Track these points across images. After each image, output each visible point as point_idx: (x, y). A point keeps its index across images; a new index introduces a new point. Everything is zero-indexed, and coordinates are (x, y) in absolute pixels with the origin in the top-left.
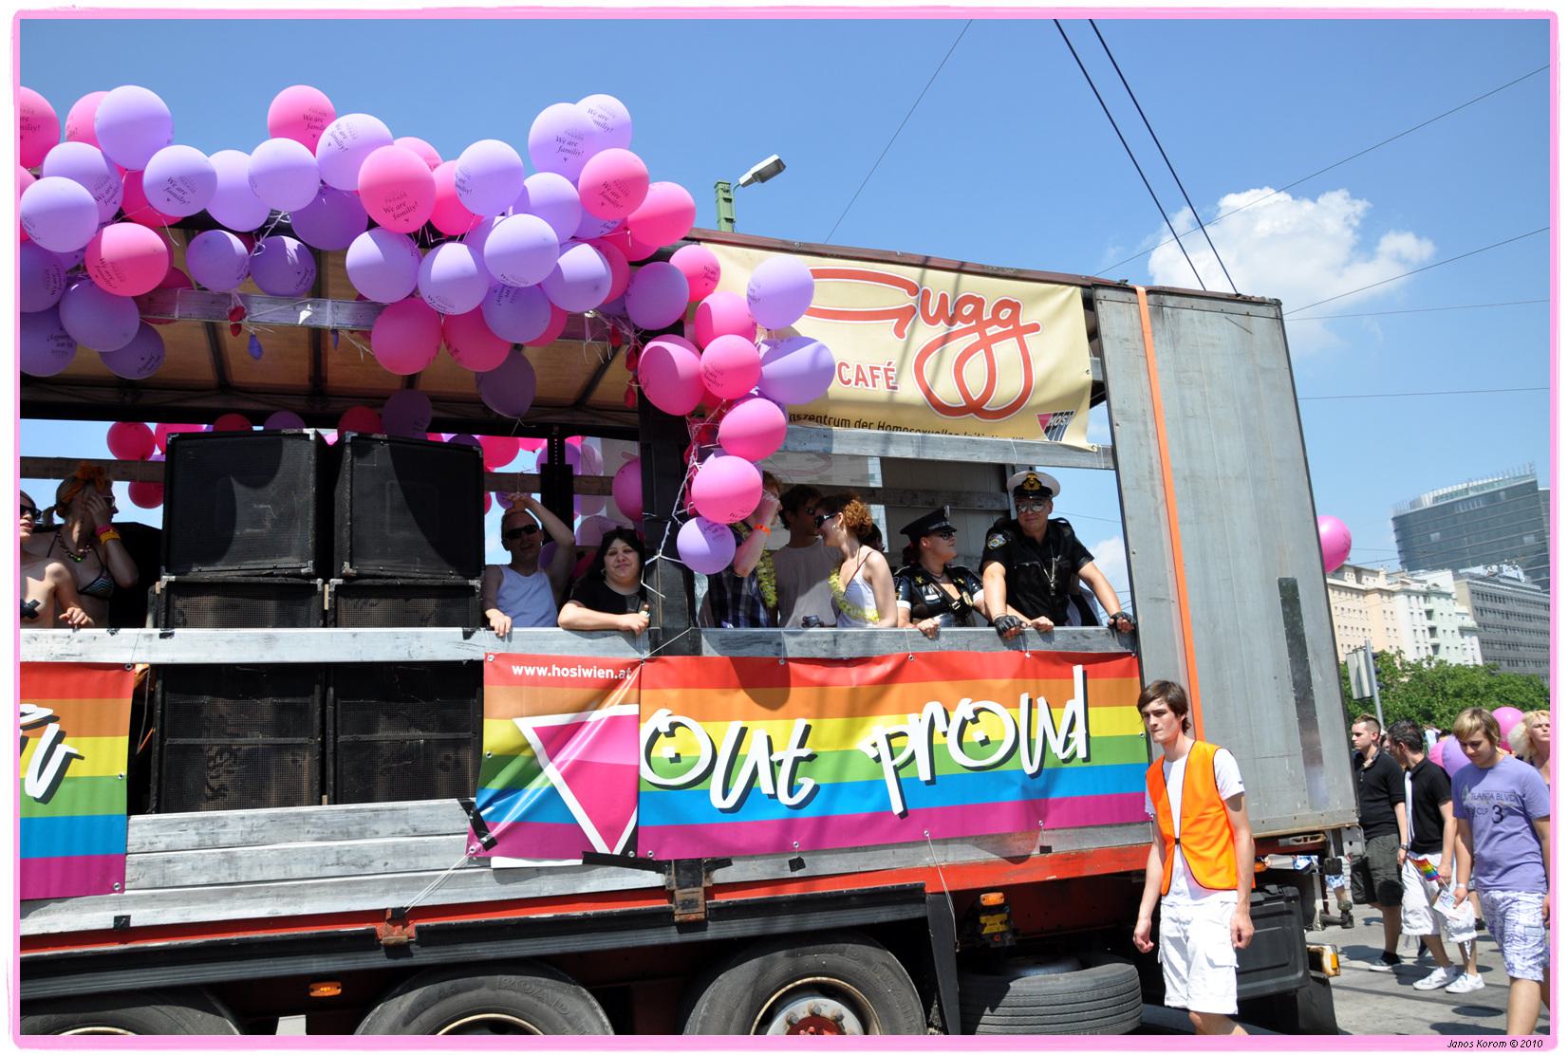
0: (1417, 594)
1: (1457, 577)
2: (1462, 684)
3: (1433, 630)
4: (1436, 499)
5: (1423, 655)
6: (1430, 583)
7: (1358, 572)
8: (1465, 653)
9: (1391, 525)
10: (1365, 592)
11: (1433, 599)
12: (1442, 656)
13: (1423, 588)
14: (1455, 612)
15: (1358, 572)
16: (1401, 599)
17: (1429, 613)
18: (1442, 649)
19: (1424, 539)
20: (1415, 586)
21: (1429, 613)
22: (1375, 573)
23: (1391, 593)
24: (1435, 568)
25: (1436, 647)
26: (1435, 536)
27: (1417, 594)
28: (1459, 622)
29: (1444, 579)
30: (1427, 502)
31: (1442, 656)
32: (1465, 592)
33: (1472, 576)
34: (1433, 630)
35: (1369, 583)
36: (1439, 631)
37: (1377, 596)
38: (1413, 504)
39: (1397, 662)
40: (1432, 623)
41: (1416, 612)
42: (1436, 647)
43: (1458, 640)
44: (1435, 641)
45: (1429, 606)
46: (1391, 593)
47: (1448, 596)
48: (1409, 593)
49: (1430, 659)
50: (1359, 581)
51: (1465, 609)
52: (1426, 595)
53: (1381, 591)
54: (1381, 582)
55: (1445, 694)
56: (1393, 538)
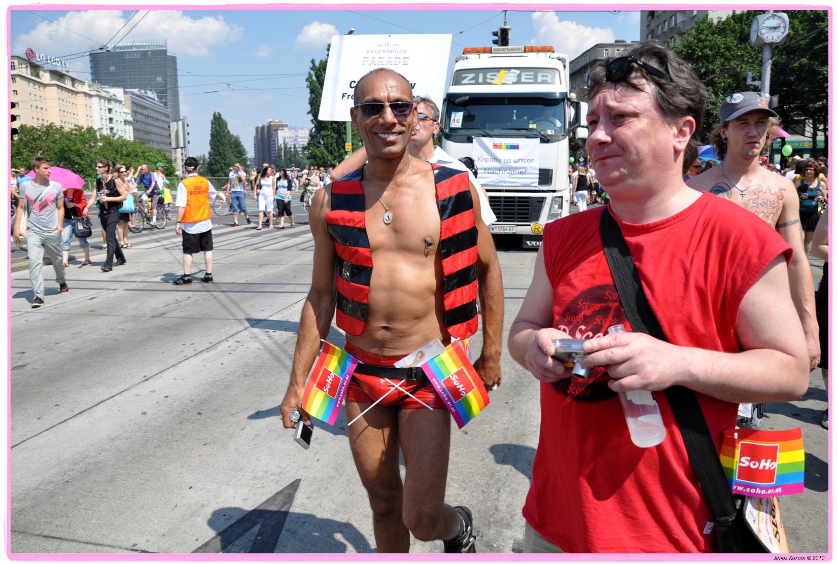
0: (105, 98)
1: (125, 93)
2: (130, 149)
3: (111, 119)
7: (73, 80)
8: (128, 134)
10: (76, 93)
11: (113, 103)
13: (108, 96)
14: (123, 112)
16: (96, 99)
17: (110, 110)
18: (115, 131)
20: (103, 94)
21: (110, 110)
22: (82, 83)
23: (91, 96)
24: (115, 85)
25: (111, 129)
27: (105, 98)
28: (122, 118)
29: (118, 92)
32: (129, 103)
33: (133, 94)
34: (111, 119)
35: (78, 88)
36: (114, 121)
40: (111, 116)
41: (103, 108)
42: (111, 129)
44: (111, 125)
45: (110, 106)
46: (91, 96)
47: (120, 102)
48: (100, 97)
50: (73, 86)
51: (128, 111)
52: (109, 100)
53: (86, 94)
54: (86, 89)
55: (122, 154)
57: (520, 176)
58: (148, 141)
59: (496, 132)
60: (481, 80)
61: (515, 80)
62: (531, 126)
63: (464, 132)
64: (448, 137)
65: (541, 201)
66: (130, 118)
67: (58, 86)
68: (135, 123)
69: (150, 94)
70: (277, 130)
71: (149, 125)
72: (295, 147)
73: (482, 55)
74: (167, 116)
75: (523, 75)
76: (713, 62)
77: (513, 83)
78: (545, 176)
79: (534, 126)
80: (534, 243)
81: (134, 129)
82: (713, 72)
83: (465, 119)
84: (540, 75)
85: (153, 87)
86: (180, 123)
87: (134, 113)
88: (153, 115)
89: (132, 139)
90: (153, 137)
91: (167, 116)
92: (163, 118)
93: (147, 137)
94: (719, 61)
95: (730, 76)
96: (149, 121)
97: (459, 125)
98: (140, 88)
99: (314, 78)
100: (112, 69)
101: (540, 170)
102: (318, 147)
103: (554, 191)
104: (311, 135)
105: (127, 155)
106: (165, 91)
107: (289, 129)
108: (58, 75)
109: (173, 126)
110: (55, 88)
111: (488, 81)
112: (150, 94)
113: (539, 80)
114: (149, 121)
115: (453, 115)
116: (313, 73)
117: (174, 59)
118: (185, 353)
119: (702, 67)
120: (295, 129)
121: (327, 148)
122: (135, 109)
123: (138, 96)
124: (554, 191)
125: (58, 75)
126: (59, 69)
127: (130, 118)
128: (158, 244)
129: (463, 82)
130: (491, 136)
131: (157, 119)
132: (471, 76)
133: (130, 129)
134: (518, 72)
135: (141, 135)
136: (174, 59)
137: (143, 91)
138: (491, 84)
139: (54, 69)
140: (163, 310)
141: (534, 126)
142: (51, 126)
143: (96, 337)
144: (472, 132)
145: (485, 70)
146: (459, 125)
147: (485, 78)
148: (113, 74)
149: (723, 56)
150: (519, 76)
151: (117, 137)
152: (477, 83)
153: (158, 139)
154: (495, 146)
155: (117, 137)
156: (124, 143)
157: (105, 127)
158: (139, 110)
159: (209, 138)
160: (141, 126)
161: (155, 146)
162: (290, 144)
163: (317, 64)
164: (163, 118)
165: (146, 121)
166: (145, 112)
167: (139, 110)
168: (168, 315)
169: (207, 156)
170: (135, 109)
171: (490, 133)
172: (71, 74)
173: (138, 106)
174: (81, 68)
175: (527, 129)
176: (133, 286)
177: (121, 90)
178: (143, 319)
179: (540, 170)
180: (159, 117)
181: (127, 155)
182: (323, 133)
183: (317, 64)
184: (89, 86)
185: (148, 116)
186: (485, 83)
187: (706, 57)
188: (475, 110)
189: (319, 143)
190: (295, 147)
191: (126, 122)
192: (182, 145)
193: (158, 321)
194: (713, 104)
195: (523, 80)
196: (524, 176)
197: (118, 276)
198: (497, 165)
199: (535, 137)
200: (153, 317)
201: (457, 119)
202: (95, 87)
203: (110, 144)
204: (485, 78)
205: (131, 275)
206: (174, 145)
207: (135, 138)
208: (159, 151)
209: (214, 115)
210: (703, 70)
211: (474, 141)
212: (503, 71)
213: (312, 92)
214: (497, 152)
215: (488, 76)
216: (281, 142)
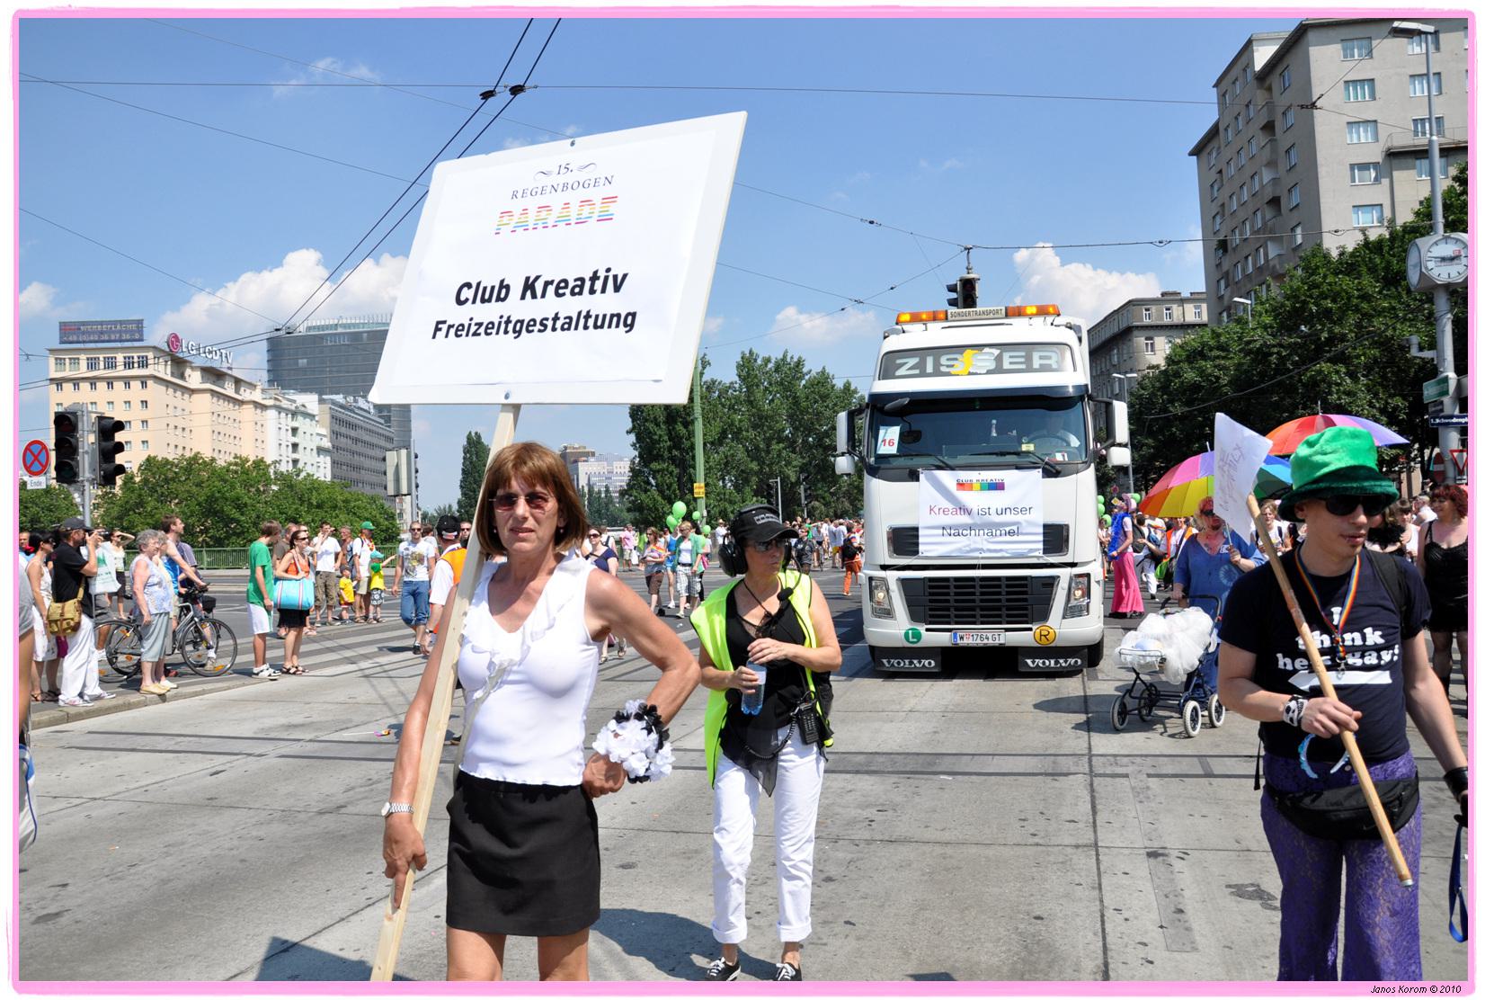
0: (287, 411)
1: (321, 401)
3: (295, 446)
6: (299, 403)
7: (238, 382)
8: (322, 470)
14: (316, 433)
16: (272, 413)
17: (295, 430)
18: (300, 465)
20: (285, 404)
21: (295, 430)
22: (252, 386)
24: (305, 389)
25: (295, 462)
28: (317, 442)
29: (310, 401)
33: (334, 403)
34: (295, 446)
35: (246, 394)
36: (300, 448)
39: (271, 471)
42: (295, 462)
44: (295, 456)
45: (295, 424)
47: (312, 417)
48: (279, 409)
50: (237, 391)
51: (324, 431)
52: (294, 414)
53: (256, 405)
54: (257, 396)
55: (310, 504)
57: (1008, 538)
58: (356, 482)
59: (962, 460)
60: (930, 369)
61: (992, 366)
62: (1024, 448)
63: (902, 462)
64: (874, 472)
65: (1050, 583)
66: (326, 443)
67: (213, 393)
68: (334, 452)
70: (576, 461)
71: (359, 454)
72: (607, 491)
73: (930, 325)
75: (1006, 356)
76: (1340, 322)
77: (989, 372)
78: (1056, 537)
79: (1031, 447)
80: (1039, 662)
81: (333, 462)
82: (1343, 338)
83: (903, 437)
84: (1036, 356)
86: (404, 452)
87: (335, 434)
89: (329, 479)
90: (365, 476)
93: (354, 475)
94: (1352, 319)
95: (1375, 344)
96: (359, 448)
97: (893, 450)
98: (346, 394)
100: (303, 362)
101: (1045, 526)
102: (646, 491)
103: (1073, 565)
104: (632, 470)
105: (319, 506)
107: (598, 460)
109: (391, 457)
110: (208, 396)
111: (943, 369)
113: (1036, 364)
114: (359, 448)
115: (882, 432)
118: (370, 892)
119: (1322, 331)
120: (607, 459)
121: (661, 492)
122: (337, 428)
123: (342, 406)
124: (1073, 565)
126: (216, 365)
127: (326, 443)
128: (353, 667)
129: (898, 373)
130: (952, 468)
131: (372, 445)
132: (913, 361)
133: (326, 461)
134: (996, 352)
135: (344, 471)
137: (351, 399)
138: (948, 374)
139: (208, 364)
140: (341, 799)
141: (1031, 447)
142: (196, 458)
143: (206, 852)
144: (916, 461)
145: (937, 351)
146: (893, 450)
147: (937, 365)
148: (304, 370)
149: (1357, 310)
150: (999, 359)
151: (303, 475)
152: (923, 374)
154: (961, 485)
155: (303, 475)
156: (315, 486)
157: (284, 459)
158: (343, 430)
159: (460, 477)
160: (346, 457)
161: (368, 491)
162: (599, 486)
164: (383, 443)
165: (354, 447)
166: (353, 433)
167: (343, 430)
168: (350, 809)
169: (455, 507)
170: (337, 428)
171: (950, 462)
172: (235, 373)
174: (251, 363)
175: (1018, 454)
176: (295, 748)
177: (315, 397)
178: (302, 816)
179: (1045, 526)
180: (375, 440)
181: (319, 506)
182: (655, 466)
184: (263, 391)
185: (356, 440)
186: (937, 373)
187: (1328, 312)
188: (920, 421)
189: (648, 483)
190: (607, 491)
191: (320, 450)
192: (404, 490)
193: (329, 822)
194: (1348, 394)
195: (1006, 366)
196: (1015, 538)
197: (270, 729)
198: (964, 519)
199: (1033, 466)
200: (320, 813)
201: (889, 439)
202: (272, 393)
203: (291, 487)
204: (937, 365)
205: (295, 726)
206: (391, 491)
207: (334, 476)
208: (373, 499)
209: (469, 437)
210: (1325, 335)
211: (922, 477)
212: (969, 352)
214: (964, 496)
215: (943, 360)
216: (583, 482)
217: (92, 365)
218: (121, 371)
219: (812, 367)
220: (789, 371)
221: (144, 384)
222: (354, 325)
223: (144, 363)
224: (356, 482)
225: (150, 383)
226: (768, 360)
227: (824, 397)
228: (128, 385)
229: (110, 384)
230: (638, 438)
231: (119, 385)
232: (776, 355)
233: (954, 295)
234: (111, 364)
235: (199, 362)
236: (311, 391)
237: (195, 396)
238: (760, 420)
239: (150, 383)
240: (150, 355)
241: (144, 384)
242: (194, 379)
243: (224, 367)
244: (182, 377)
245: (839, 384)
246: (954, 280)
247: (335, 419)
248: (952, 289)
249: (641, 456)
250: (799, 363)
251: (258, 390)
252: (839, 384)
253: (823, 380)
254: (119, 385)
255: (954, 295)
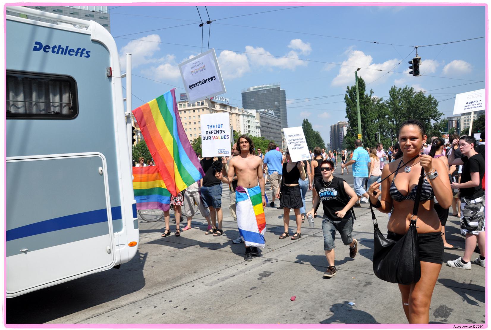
0: (246, 115)
1: (257, 112)
4: (254, 89)
5: (246, 133)
7: (231, 107)
8: (256, 133)
9: (241, 96)
12: (251, 134)
14: (256, 122)
15: (231, 107)
16: (241, 117)
18: (251, 132)
19: (249, 100)
20: (245, 113)
21: (249, 121)
22: (235, 108)
23: (239, 115)
24: (252, 109)
25: (249, 131)
26: (253, 100)
28: (256, 125)
29: (253, 112)
30: (252, 89)
31: (251, 134)
32: (259, 116)
33: (261, 112)
34: (249, 126)
35: (233, 111)
37: (235, 115)
38: (248, 90)
43: (255, 130)
44: (249, 129)
45: (249, 119)
46: (239, 115)
47: (254, 117)
48: (244, 115)
49: (248, 134)
50: (231, 110)
51: (258, 121)
52: (248, 116)
53: (236, 114)
54: (237, 111)
56: (241, 99)
58: (268, 137)
66: (259, 125)
69: (270, 112)
74: (279, 123)
81: (261, 131)
85: (271, 108)
87: (261, 122)
88: (272, 122)
89: (260, 136)
90: (272, 134)
91: (279, 123)
92: (277, 124)
93: (268, 134)
96: (270, 126)
98: (265, 108)
99: (349, 97)
106: (279, 110)
108: (223, 106)
112: (270, 112)
114: (270, 126)
116: (348, 94)
117: (284, 92)
122: (262, 120)
125: (223, 106)
126: (224, 103)
127: (259, 125)
131: (273, 125)
135: (265, 133)
136: (284, 92)
153: (274, 135)
158: (264, 120)
161: (272, 139)
163: (350, 89)
164: (277, 124)
165: (268, 126)
166: (267, 121)
167: (264, 120)
170: (262, 120)
173: (263, 119)
180: (274, 123)
183: (350, 89)
185: (268, 123)
191: (257, 127)
207: (261, 135)
213: (348, 105)
217: (189, 106)
218: (197, 107)
219: (417, 90)
220: (408, 93)
221: (203, 110)
222: (266, 87)
223: (203, 104)
224: (268, 137)
225: (205, 109)
226: (400, 89)
227: (421, 101)
228: (199, 111)
229: (194, 111)
230: (349, 118)
231: (196, 111)
232: (403, 87)
233: (411, 65)
234: (194, 105)
235: (219, 102)
236: (253, 109)
237: (219, 113)
238: (396, 110)
239: (205, 109)
240: (205, 101)
241: (203, 110)
242: (218, 107)
243: (226, 104)
244: (214, 107)
245: (427, 96)
246: (411, 59)
247: (261, 117)
248: (410, 63)
249: (350, 125)
250: (412, 90)
251: (237, 109)
252: (427, 96)
253: (420, 94)
254: (196, 111)
255: (411, 65)
